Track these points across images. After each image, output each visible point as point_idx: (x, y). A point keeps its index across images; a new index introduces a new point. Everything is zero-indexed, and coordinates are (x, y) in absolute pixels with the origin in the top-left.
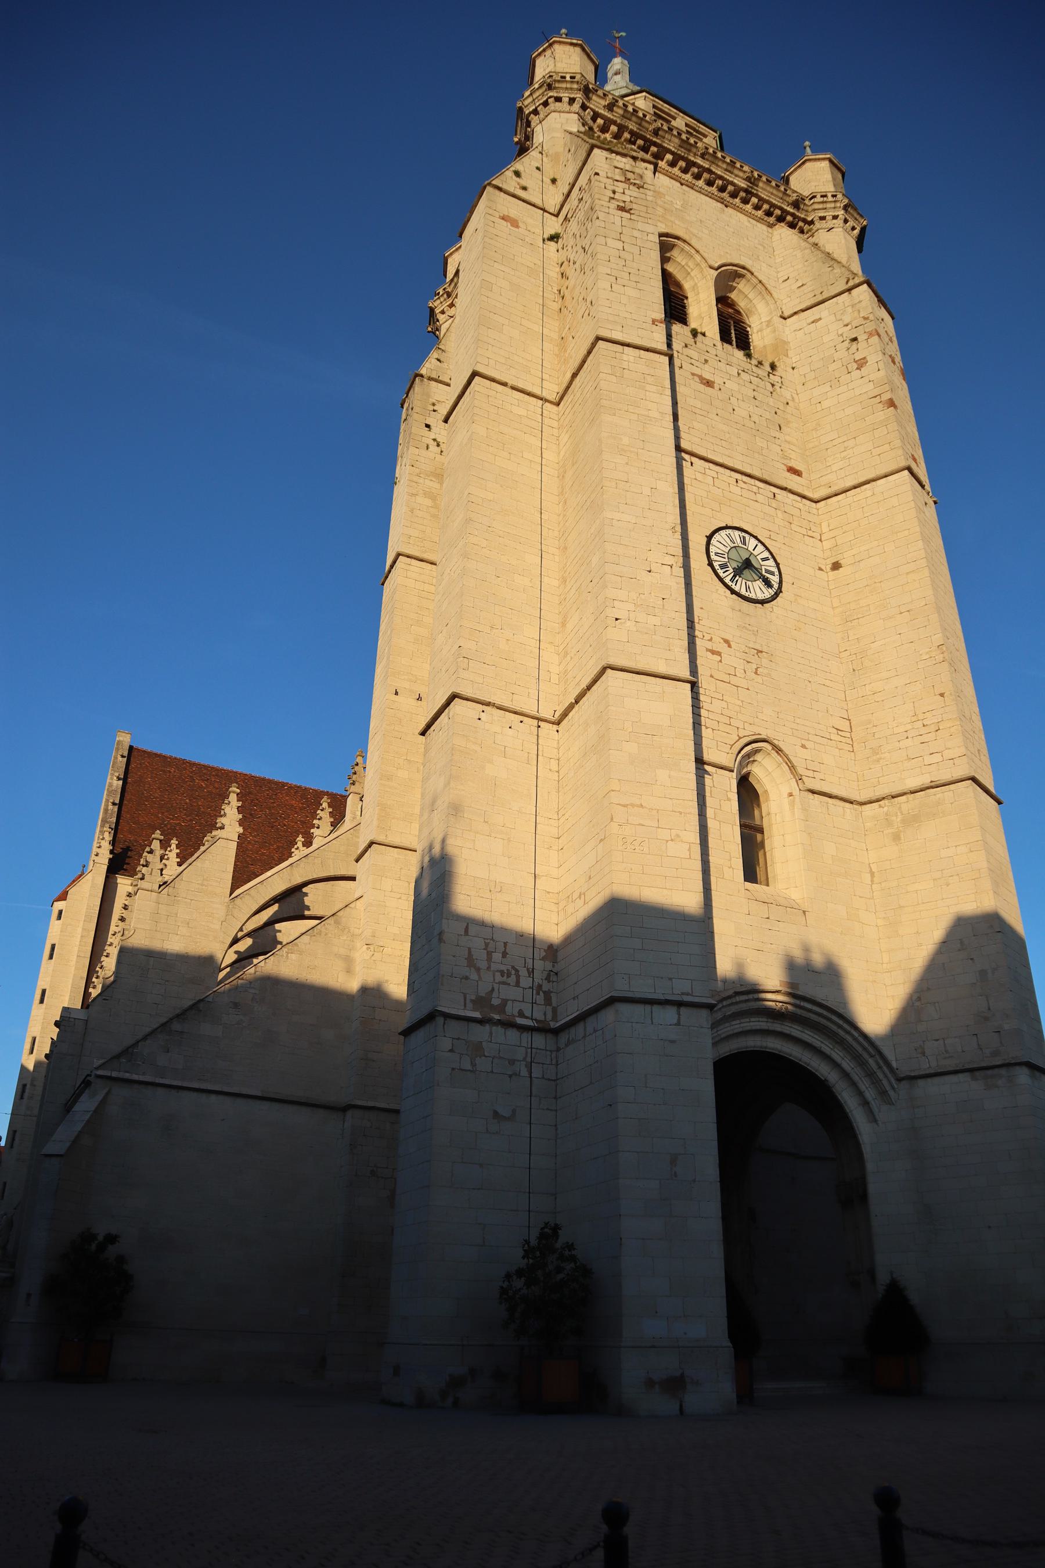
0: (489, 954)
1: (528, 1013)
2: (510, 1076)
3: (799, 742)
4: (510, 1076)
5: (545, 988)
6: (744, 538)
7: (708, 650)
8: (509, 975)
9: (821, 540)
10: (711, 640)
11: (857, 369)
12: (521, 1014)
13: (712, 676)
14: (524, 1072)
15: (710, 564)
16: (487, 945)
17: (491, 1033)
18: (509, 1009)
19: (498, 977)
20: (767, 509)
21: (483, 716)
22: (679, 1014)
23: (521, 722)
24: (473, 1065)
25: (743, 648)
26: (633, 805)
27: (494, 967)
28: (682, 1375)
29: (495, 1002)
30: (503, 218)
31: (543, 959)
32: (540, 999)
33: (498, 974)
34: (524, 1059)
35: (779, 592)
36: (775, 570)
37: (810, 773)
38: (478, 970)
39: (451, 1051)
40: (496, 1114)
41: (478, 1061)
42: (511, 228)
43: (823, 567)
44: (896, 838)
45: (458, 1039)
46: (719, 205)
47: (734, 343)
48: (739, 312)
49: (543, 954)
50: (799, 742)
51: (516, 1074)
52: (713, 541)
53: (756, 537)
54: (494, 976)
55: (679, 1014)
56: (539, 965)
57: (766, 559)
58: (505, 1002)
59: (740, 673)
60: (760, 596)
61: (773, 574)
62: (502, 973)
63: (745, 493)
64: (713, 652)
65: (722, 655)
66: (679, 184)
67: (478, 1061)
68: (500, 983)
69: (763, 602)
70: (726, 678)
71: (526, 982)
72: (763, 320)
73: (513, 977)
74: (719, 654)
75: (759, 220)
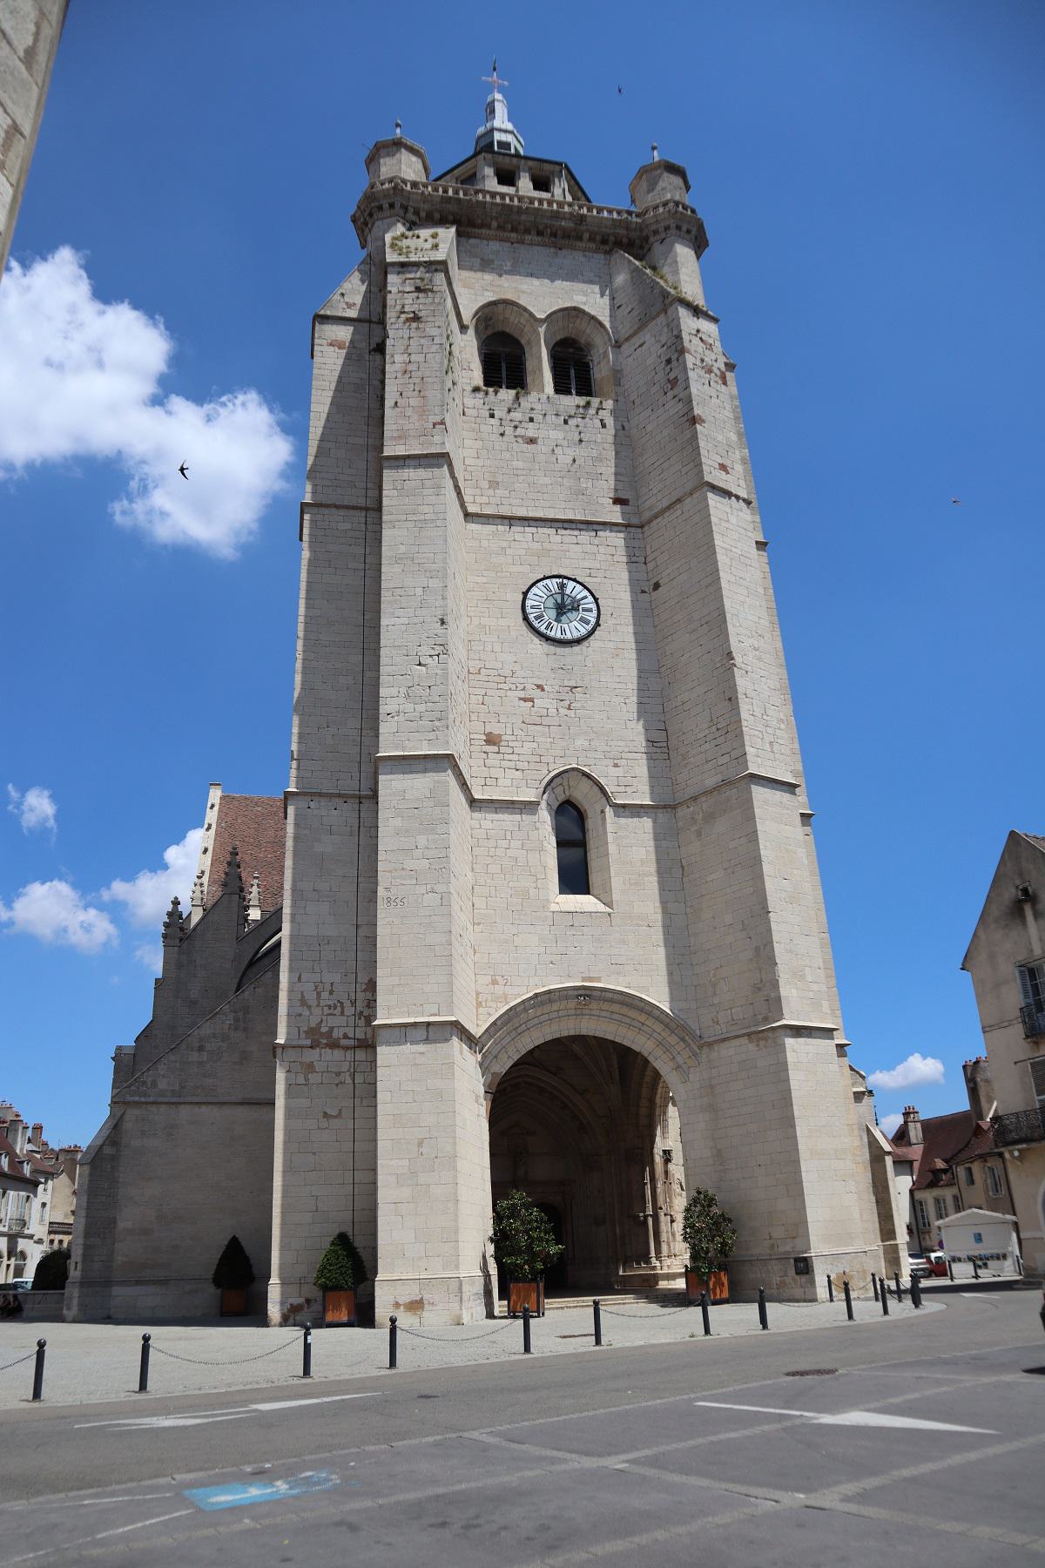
0: (319, 995)
1: (351, 1035)
2: (337, 1085)
3: (611, 763)
4: (337, 1085)
7: (520, 699)
8: (335, 1008)
9: (645, 563)
10: (524, 689)
11: (671, 389)
12: (346, 1036)
13: (523, 722)
14: (349, 1081)
15: (526, 618)
16: (316, 987)
18: (335, 1034)
19: (326, 1010)
20: (589, 548)
21: (312, 805)
22: (428, 1032)
23: (345, 802)
24: (306, 1079)
25: (557, 688)
26: (396, 870)
28: (422, 1299)
29: (324, 1030)
30: (331, 345)
31: (365, 991)
32: (362, 1022)
34: (349, 1070)
35: (598, 624)
36: (593, 606)
37: (622, 789)
38: (309, 1007)
40: (325, 1113)
42: (340, 351)
43: (646, 589)
44: (699, 833)
45: (294, 1062)
46: (552, 250)
48: (581, 349)
50: (611, 763)
51: (341, 1083)
52: (530, 595)
53: (575, 580)
54: (323, 1009)
55: (428, 1032)
56: (361, 996)
57: (586, 597)
58: (332, 1029)
59: (553, 711)
60: (576, 635)
61: (590, 610)
62: (329, 1007)
63: (567, 539)
64: (525, 700)
65: (535, 700)
66: (509, 244)
69: (579, 641)
70: (538, 720)
71: (349, 1010)
72: (601, 352)
73: (339, 1008)
74: (532, 700)
75: (596, 251)
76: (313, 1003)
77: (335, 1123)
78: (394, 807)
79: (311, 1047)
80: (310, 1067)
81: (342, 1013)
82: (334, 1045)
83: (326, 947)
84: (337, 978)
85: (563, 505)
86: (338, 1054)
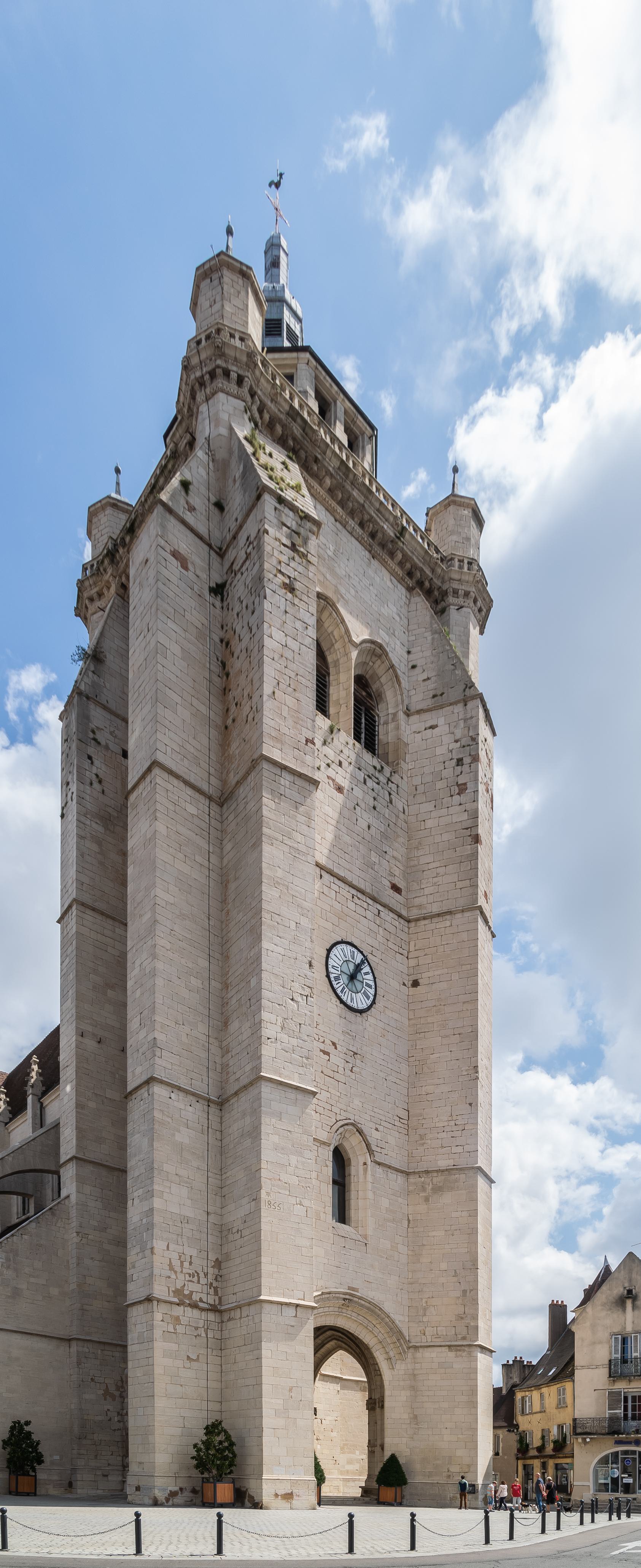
0: (182, 1263)
5: (214, 1285)
6: (354, 952)
12: (201, 1300)
15: (328, 976)
16: (180, 1257)
17: (184, 1311)
24: (175, 1329)
27: (185, 1271)
29: (186, 1292)
33: (187, 1276)
38: (176, 1272)
39: (162, 1321)
41: (177, 1327)
47: (363, 740)
49: (213, 1264)
52: (332, 955)
56: (211, 1271)
58: (192, 1292)
67: (177, 1327)
68: (188, 1281)
71: (203, 1281)
73: (196, 1279)
76: (178, 1269)
77: (195, 1365)
78: (273, 1125)
79: (178, 1305)
80: (177, 1320)
81: (199, 1282)
82: (194, 1306)
83: (186, 1225)
84: (194, 1252)
85: (358, 872)
86: (196, 1313)
